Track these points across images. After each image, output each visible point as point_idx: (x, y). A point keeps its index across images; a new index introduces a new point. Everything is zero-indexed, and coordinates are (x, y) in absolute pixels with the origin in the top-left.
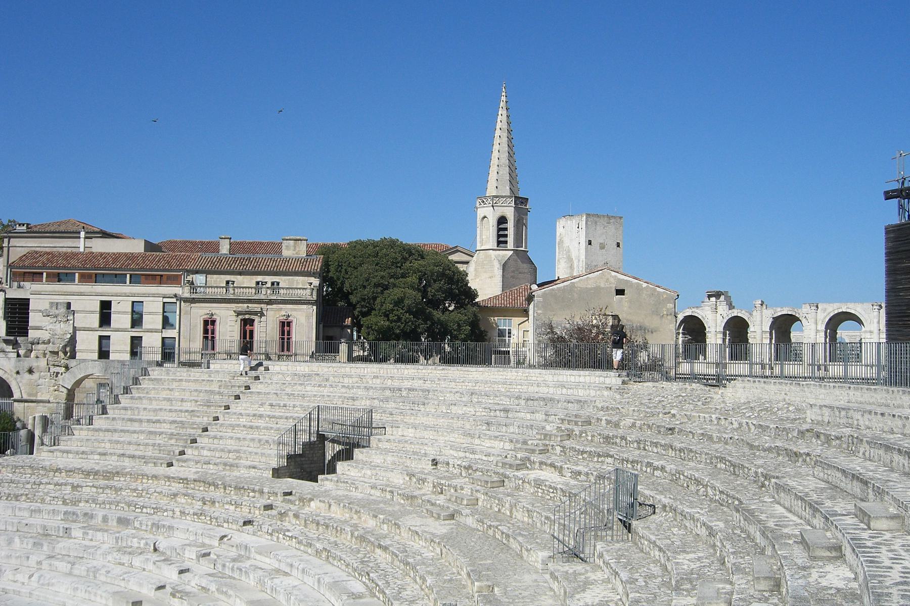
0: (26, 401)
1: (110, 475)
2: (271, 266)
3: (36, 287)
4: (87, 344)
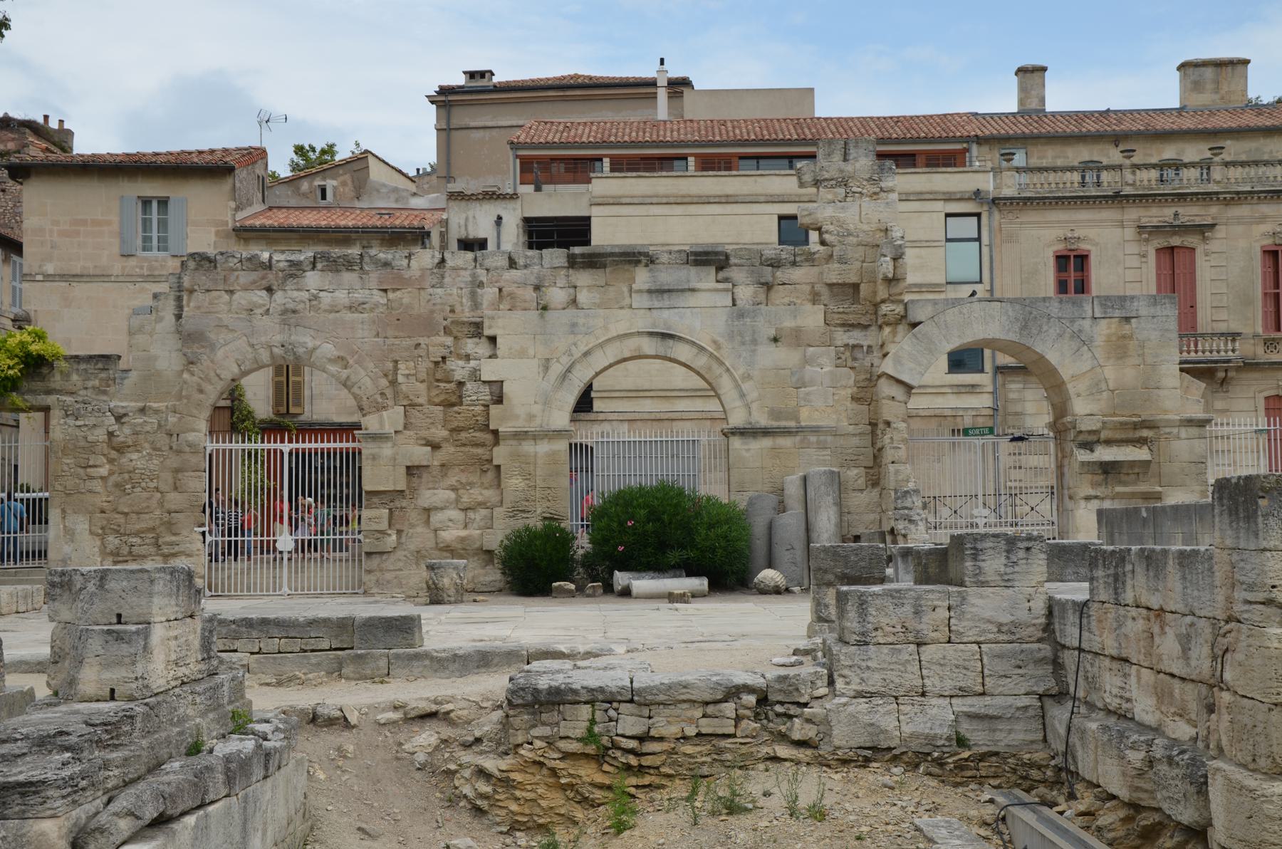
0: (766, 432)
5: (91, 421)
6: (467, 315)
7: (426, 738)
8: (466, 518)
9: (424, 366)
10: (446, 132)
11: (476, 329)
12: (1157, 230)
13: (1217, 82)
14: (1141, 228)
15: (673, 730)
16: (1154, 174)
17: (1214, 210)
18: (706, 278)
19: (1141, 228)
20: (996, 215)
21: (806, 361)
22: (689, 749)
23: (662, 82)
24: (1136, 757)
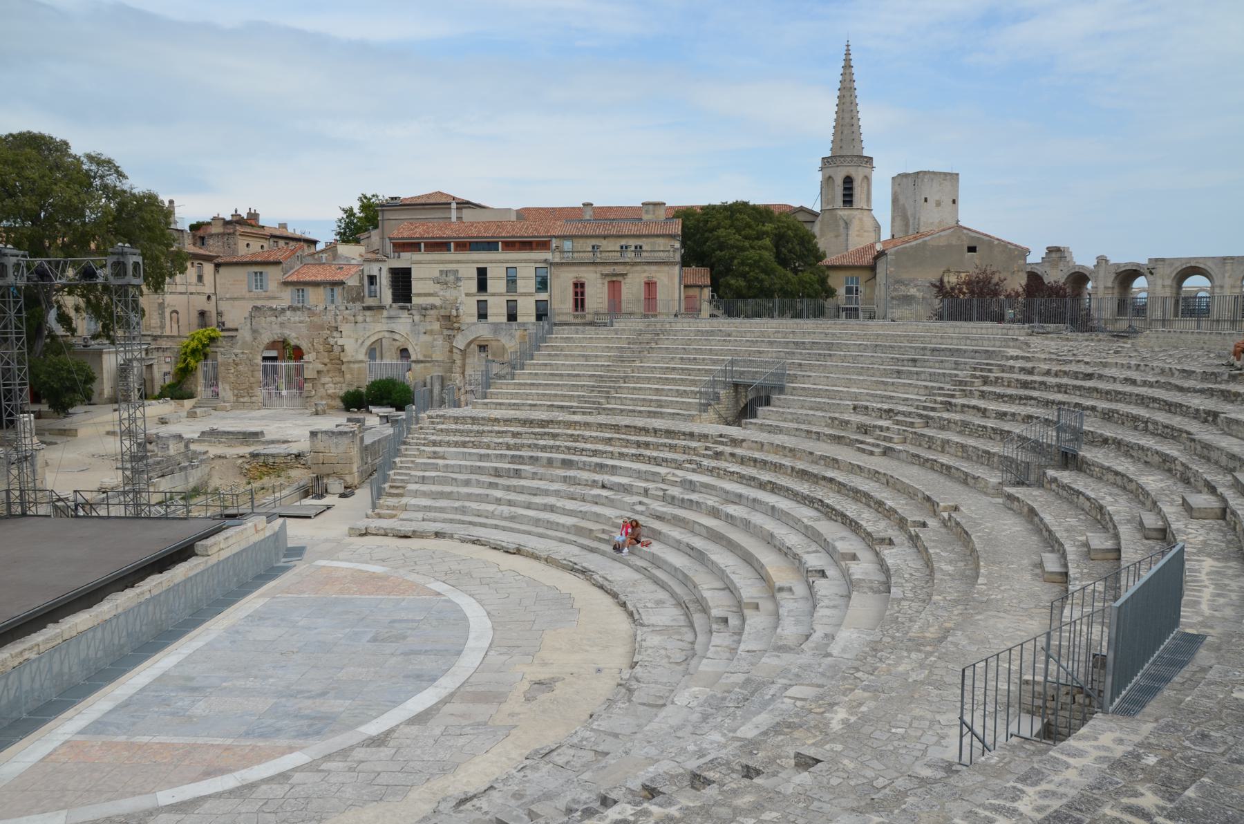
1: (544, 423)
2: (634, 230)
3: (416, 256)
4: (469, 308)
6: (334, 324)
7: (240, 461)
8: (335, 387)
11: (336, 329)
12: (607, 275)
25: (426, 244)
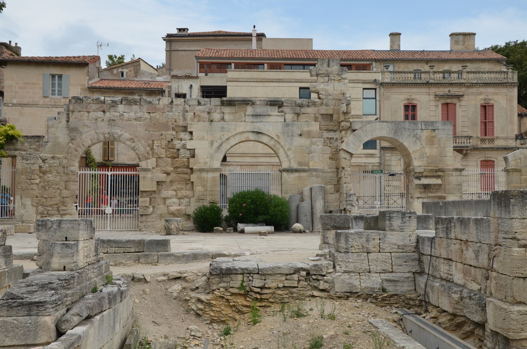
0: (296, 171)
5: (32, 162)
6: (181, 123)
7: (177, 287)
8: (180, 202)
9: (164, 142)
10: (169, 52)
11: (185, 129)
12: (442, 97)
13: (464, 41)
14: (436, 96)
15: (274, 285)
16: (441, 75)
17: (463, 89)
18: (274, 111)
19: (436, 96)
20: (382, 89)
21: (312, 144)
22: (280, 292)
23: (254, 35)
24: (456, 296)
25: (235, 63)
